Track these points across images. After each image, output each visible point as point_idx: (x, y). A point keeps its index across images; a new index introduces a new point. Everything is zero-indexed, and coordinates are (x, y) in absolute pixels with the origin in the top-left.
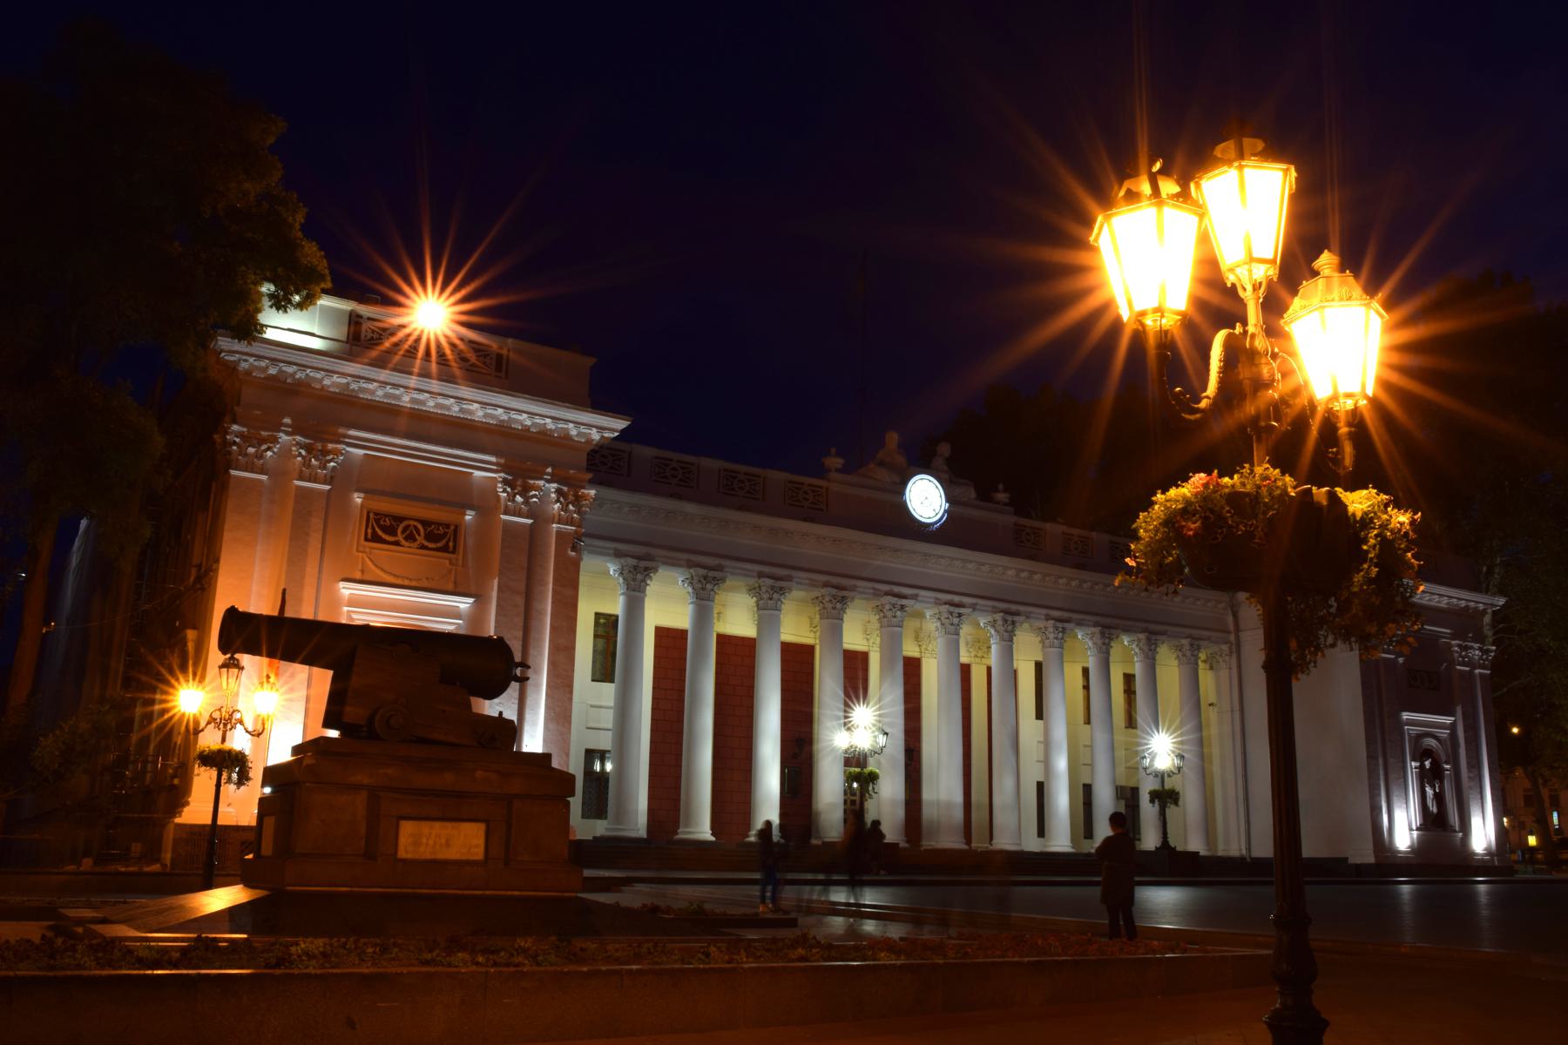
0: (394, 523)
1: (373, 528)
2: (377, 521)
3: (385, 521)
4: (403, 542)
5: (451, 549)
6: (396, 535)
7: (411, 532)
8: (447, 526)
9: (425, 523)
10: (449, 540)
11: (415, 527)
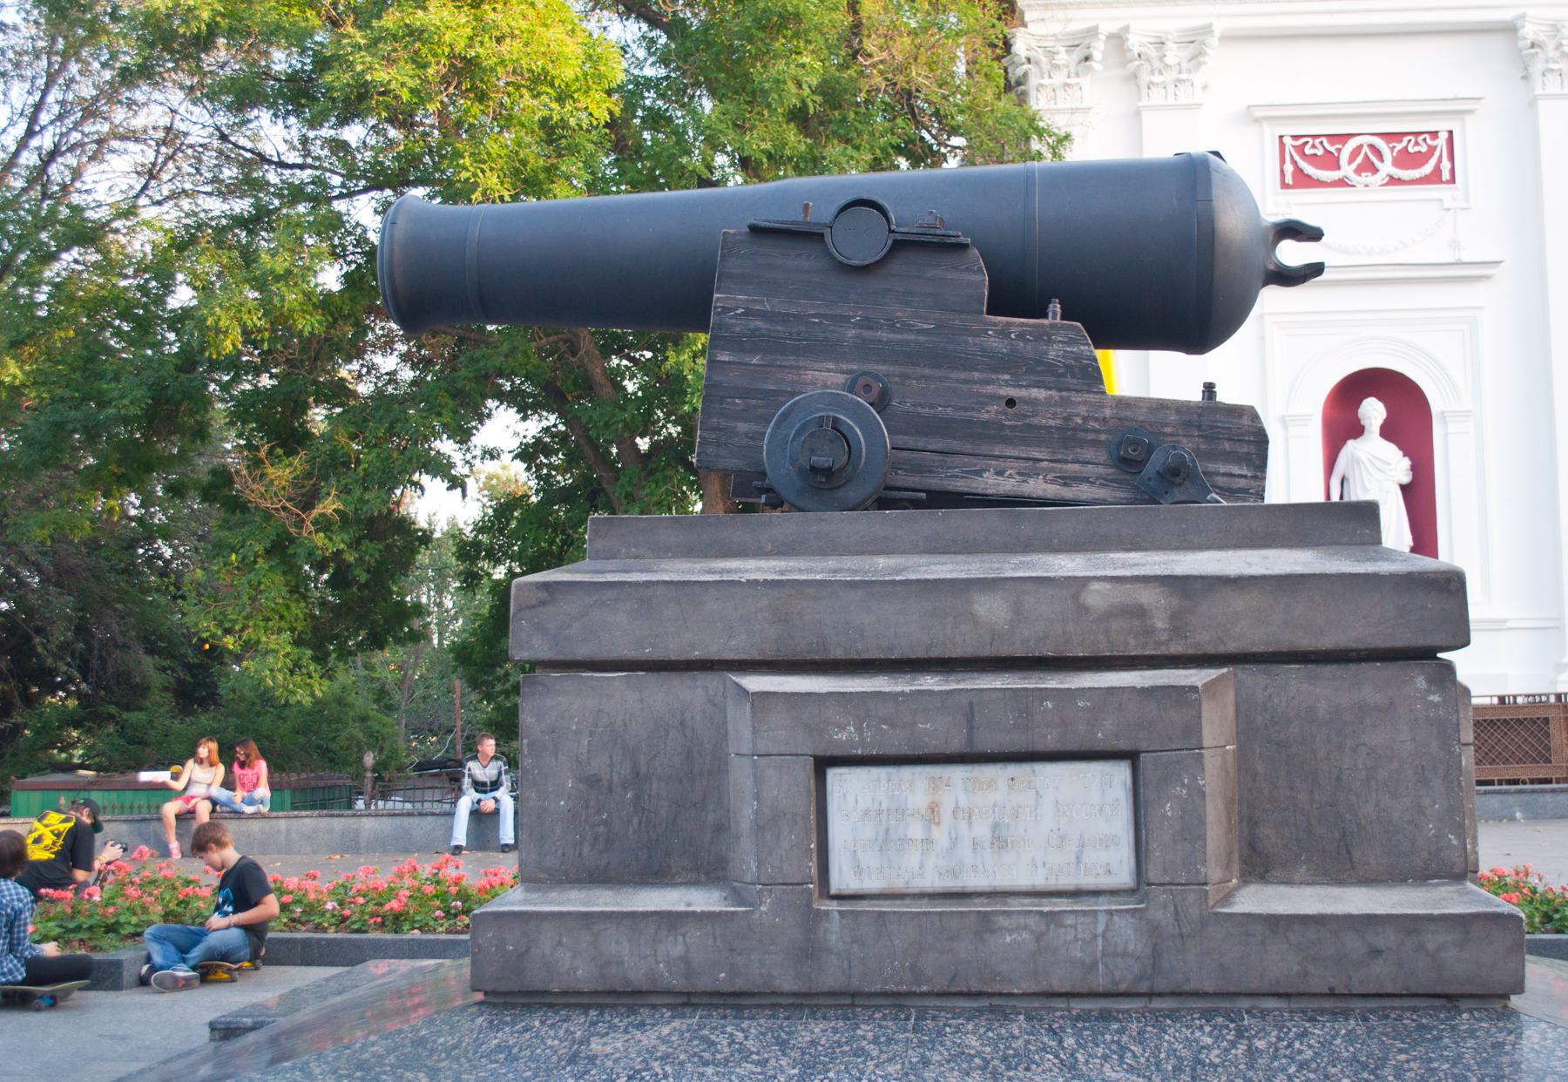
1: (1294, 162)
2: (1300, 149)
3: (1314, 146)
4: (1354, 178)
5: (1446, 176)
6: (1336, 166)
7: (1366, 154)
8: (1434, 134)
9: (1389, 137)
10: (1440, 158)
11: (1372, 147)
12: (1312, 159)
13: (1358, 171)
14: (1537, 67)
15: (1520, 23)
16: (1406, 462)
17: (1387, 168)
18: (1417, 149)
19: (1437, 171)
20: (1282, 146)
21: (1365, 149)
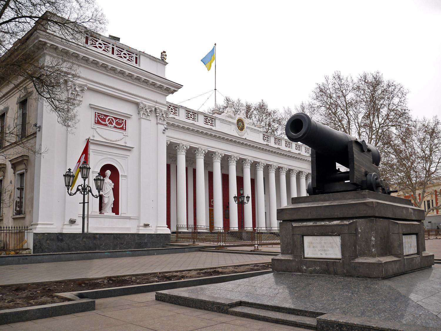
2: (99, 116)
5: (124, 129)
6: (105, 122)
8: (123, 120)
9: (116, 118)
10: (124, 124)
11: (112, 119)
12: (101, 118)
13: (109, 123)
14: (142, 113)
17: (114, 124)
18: (120, 122)
19: (123, 127)
20: (95, 114)
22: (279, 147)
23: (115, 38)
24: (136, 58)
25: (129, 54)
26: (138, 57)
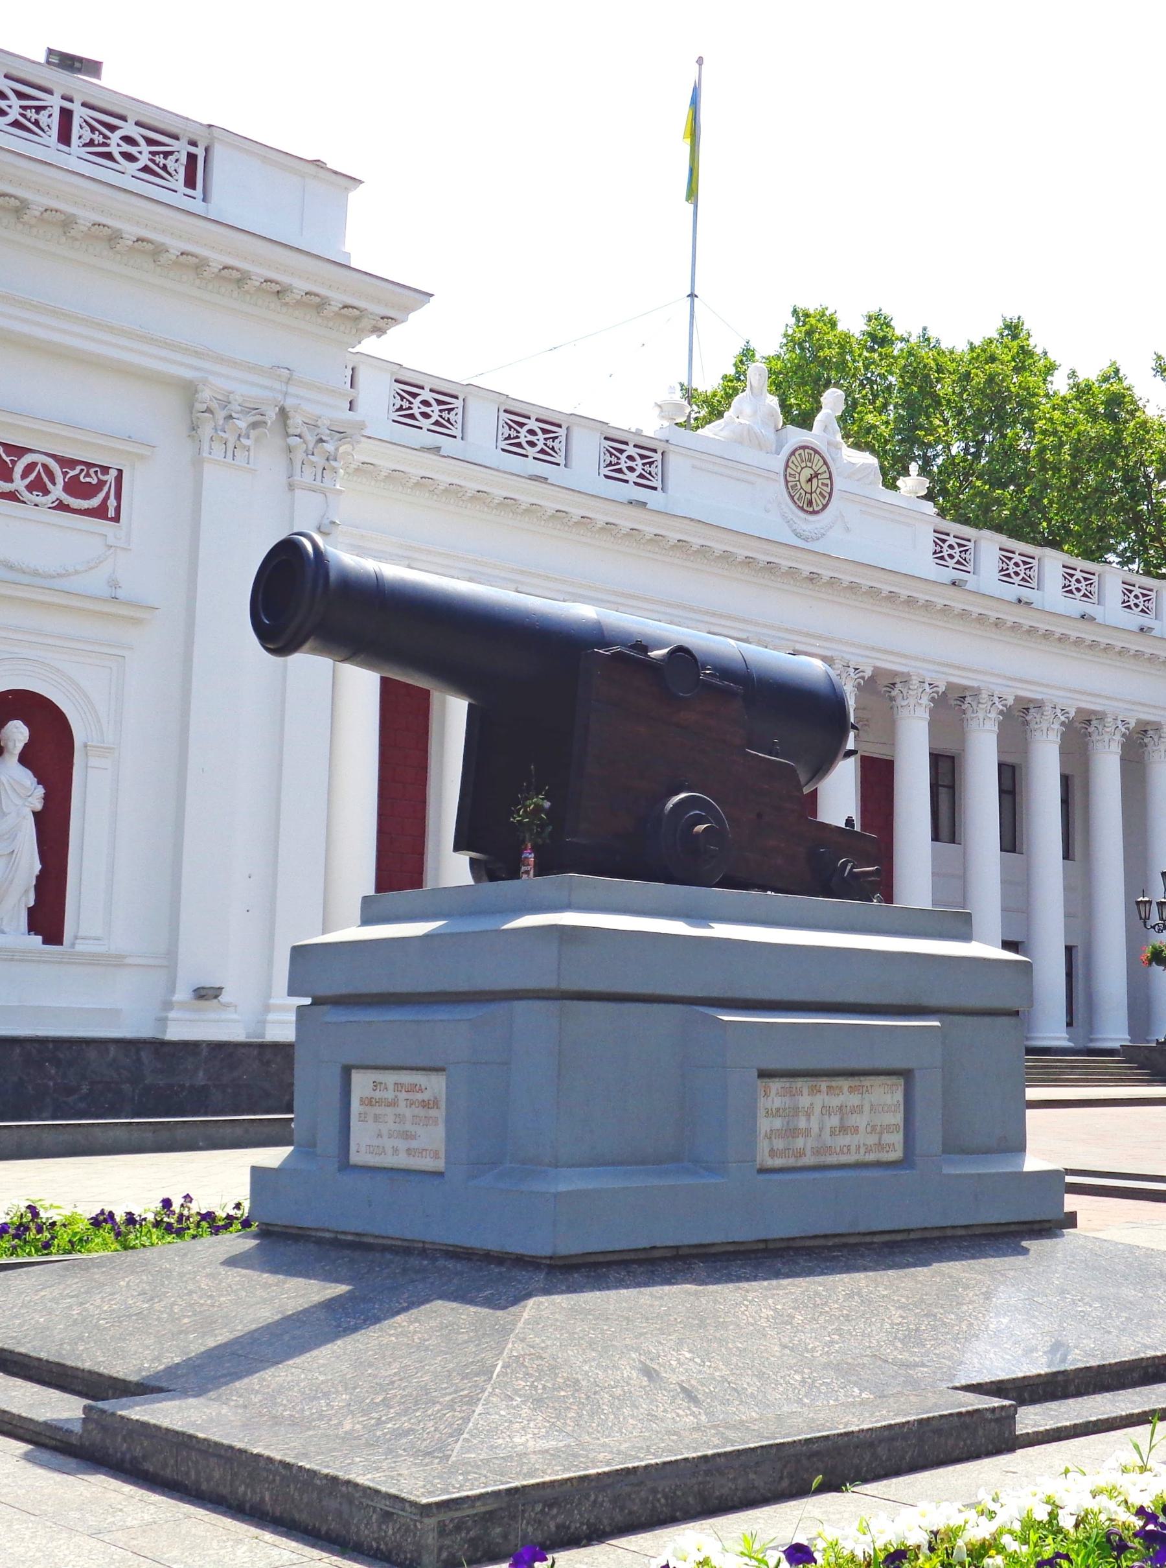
0: (7, 459)
4: (26, 495)
8: (105, 470)
9: (67, 463)
10: (108, 493)
11: (45, 466)
13: (30, 488)
15: (201, 387)
16: (40, 791)
17: (57, 491)
18: (88, 480)
21: (40, 465)
22: (1025, 593)
23: (77, 65)
24: (192, 158)
25: (150, 142)
26: (200, 152)
